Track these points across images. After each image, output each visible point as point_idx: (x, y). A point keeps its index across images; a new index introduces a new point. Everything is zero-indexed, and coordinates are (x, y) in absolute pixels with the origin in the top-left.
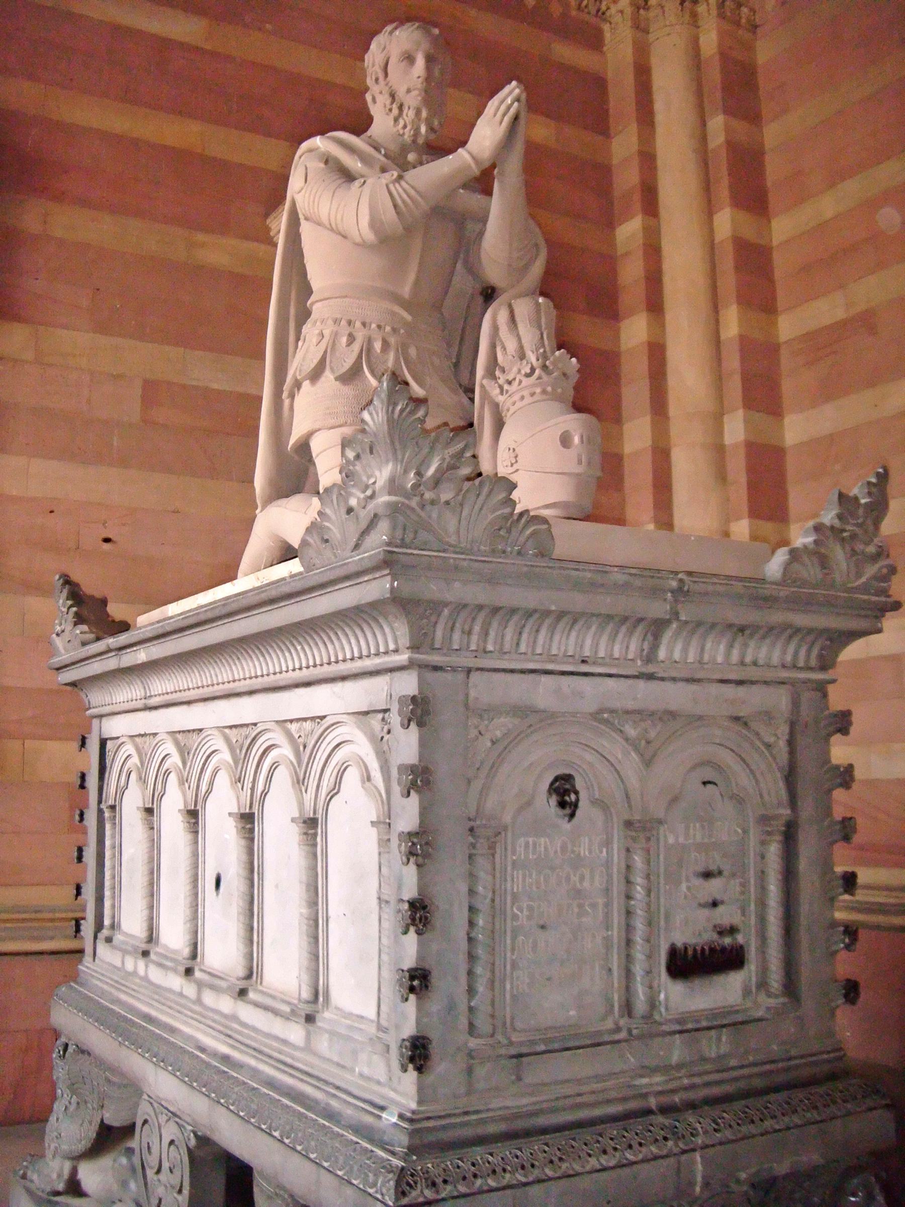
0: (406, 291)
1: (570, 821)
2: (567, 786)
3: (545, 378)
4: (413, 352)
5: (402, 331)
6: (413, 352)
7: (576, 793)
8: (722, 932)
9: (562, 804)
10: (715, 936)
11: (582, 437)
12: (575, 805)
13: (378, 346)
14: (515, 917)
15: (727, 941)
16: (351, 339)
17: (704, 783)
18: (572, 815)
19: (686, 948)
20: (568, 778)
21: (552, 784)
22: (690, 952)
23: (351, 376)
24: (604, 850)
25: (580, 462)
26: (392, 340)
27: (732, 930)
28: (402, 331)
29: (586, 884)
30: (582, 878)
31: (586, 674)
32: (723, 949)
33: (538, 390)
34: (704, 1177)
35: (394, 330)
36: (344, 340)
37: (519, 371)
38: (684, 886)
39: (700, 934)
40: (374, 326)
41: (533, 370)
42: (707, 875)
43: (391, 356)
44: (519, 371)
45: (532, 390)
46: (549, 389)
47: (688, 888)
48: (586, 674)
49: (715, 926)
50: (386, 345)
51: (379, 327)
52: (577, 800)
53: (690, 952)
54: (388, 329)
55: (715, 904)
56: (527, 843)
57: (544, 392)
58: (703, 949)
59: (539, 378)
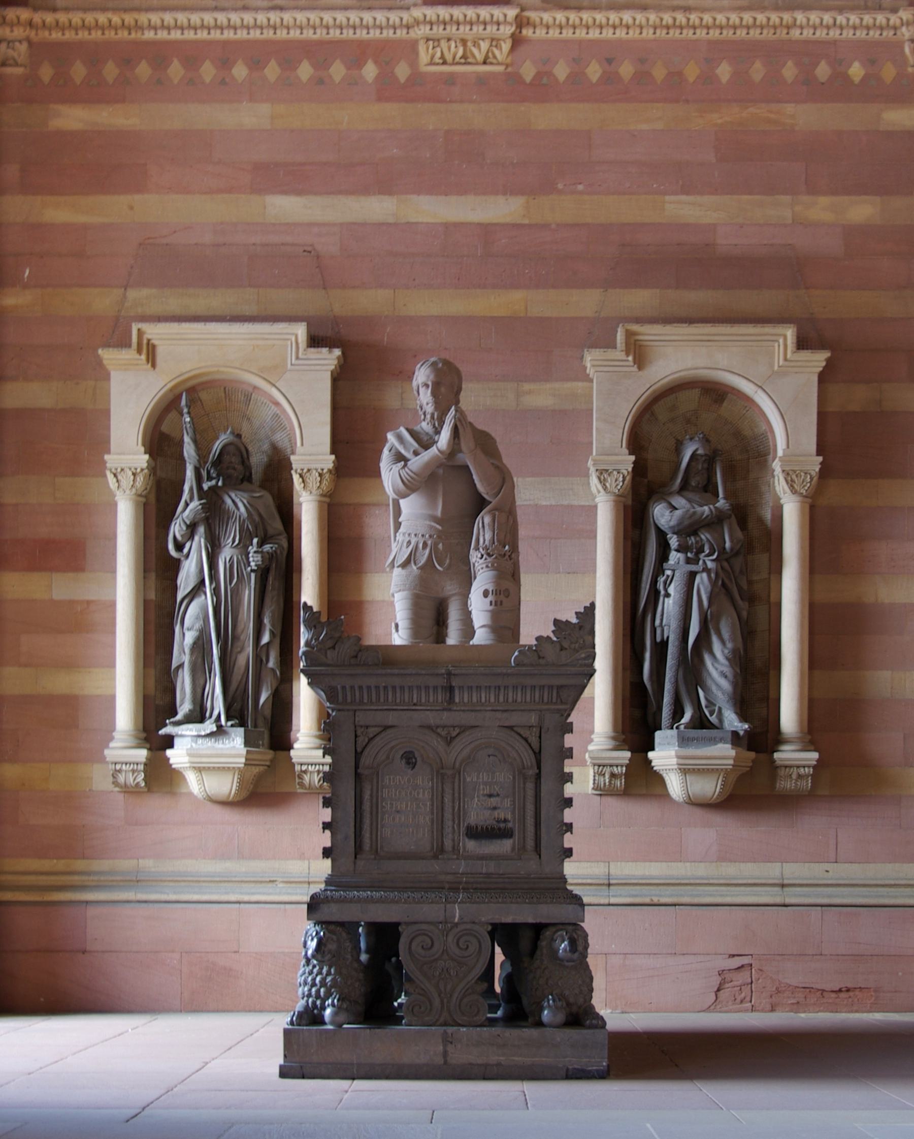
0: (439, 513)
1: (412, 770)
2: (411, 756)
3: (489, 559)
4: (440, 546)
5: (435, 536)
6: (440, 546)
7: (416, 759)
8: (498, 821)
9: (408, 763)
10: (495, 823)
11: (493, 591)
12: (415, 763)
13: (421, 545)
14: (384, 807)
15: (502, 825)
16: (409, 542)
17: (489, 756)
18: (413, 768)
19: (477, 827)
20: (411, 752)
21: (402, 755)
22: (480, 828)
23: (405, 565)
24: (430, 783)
25: (491, 604)
26: (429, 542)
27: (505, 821)
28: (435, 536)
29: (421, 796)
30: (418, 794)
31: (413, 710)
32: (500, 829)
33: (484, 566)
34: (460, 916)
35: (430, 536)
36: (405, 544)
37: (477, 557)
38: (476, 799)
39: (486, 821)
40: (420, 535)
41: (482, 556)
42: (490, 796)
43: (427, 551)
44: (477, 557)
45: (482, 566)
46: (490, 565)
47: (478, 801)
48: (413, 710)
49: (495, 818)
50: (425, 545)
51: (423, 536)
52: (416, 762)
53: (480, 828)
54: (427, 536)
55: (495, 808)
56: (390, 779)
57: (487, 567)
58: (482, 828)
59: (486, 559)
